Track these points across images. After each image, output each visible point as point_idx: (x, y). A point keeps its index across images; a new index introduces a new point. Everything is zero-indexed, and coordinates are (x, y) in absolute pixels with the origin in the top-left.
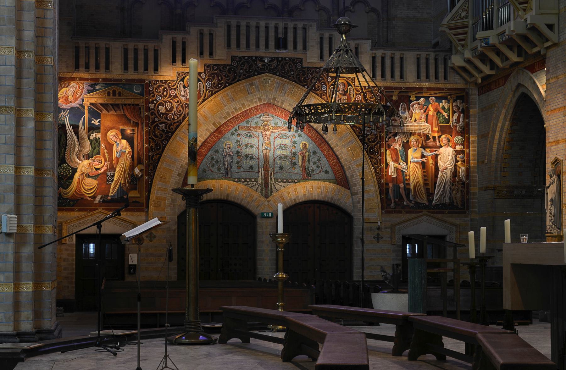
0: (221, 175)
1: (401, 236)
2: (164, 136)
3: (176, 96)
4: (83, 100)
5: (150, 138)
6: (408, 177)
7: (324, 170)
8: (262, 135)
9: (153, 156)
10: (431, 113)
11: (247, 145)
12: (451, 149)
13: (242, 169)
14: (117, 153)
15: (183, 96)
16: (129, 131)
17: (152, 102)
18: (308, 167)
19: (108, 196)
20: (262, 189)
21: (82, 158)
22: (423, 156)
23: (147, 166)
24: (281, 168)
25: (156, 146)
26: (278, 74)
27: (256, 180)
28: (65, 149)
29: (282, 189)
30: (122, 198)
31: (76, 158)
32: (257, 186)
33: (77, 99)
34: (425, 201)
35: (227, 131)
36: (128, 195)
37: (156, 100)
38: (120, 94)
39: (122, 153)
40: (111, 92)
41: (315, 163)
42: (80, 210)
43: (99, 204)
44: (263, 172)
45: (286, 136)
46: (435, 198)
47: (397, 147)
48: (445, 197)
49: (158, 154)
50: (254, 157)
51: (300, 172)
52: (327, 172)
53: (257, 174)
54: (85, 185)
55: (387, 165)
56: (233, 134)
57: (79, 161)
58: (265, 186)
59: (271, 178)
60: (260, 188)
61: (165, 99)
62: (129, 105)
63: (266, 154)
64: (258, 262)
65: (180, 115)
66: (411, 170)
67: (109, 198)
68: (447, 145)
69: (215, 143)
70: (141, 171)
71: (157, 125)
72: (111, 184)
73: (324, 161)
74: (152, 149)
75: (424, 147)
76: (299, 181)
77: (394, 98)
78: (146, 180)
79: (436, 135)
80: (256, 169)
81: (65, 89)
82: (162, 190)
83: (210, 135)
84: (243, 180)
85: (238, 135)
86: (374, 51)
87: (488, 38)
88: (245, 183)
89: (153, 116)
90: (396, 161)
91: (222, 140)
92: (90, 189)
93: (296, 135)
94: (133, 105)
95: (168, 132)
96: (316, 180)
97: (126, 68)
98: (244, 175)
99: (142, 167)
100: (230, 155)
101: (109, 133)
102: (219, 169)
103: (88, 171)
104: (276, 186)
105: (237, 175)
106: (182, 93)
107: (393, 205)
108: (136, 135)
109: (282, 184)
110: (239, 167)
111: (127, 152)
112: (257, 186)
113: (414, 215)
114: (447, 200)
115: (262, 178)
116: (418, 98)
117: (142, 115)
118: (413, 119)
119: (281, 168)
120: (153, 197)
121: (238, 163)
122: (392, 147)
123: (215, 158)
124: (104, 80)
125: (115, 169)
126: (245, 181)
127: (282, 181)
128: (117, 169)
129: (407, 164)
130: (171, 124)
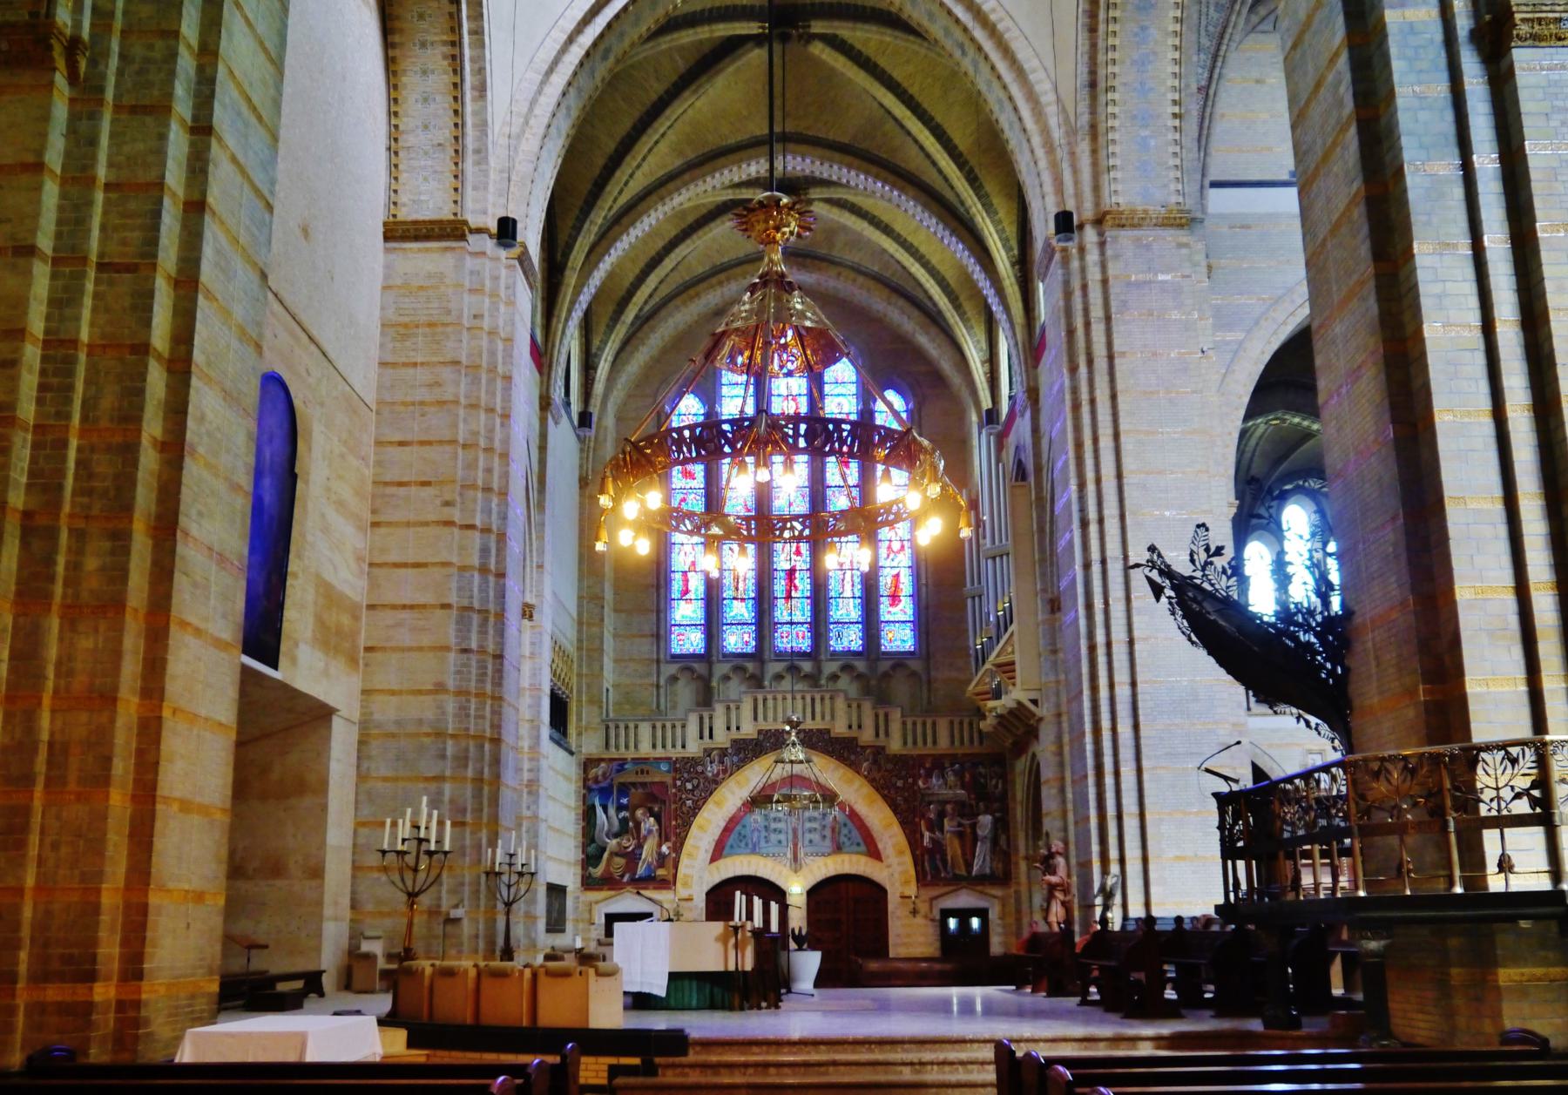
22: (960, 825)
23: (675, 844)
34: (964, 873)
39: (650, 832)
55: (922, 836)
68: (986, 812)
73: (855, 833)
75: (962, 816)
90: (931, 829)
97: (654, 746)
98: (771, 850)
114: (988, 871)
116: (952, 765)
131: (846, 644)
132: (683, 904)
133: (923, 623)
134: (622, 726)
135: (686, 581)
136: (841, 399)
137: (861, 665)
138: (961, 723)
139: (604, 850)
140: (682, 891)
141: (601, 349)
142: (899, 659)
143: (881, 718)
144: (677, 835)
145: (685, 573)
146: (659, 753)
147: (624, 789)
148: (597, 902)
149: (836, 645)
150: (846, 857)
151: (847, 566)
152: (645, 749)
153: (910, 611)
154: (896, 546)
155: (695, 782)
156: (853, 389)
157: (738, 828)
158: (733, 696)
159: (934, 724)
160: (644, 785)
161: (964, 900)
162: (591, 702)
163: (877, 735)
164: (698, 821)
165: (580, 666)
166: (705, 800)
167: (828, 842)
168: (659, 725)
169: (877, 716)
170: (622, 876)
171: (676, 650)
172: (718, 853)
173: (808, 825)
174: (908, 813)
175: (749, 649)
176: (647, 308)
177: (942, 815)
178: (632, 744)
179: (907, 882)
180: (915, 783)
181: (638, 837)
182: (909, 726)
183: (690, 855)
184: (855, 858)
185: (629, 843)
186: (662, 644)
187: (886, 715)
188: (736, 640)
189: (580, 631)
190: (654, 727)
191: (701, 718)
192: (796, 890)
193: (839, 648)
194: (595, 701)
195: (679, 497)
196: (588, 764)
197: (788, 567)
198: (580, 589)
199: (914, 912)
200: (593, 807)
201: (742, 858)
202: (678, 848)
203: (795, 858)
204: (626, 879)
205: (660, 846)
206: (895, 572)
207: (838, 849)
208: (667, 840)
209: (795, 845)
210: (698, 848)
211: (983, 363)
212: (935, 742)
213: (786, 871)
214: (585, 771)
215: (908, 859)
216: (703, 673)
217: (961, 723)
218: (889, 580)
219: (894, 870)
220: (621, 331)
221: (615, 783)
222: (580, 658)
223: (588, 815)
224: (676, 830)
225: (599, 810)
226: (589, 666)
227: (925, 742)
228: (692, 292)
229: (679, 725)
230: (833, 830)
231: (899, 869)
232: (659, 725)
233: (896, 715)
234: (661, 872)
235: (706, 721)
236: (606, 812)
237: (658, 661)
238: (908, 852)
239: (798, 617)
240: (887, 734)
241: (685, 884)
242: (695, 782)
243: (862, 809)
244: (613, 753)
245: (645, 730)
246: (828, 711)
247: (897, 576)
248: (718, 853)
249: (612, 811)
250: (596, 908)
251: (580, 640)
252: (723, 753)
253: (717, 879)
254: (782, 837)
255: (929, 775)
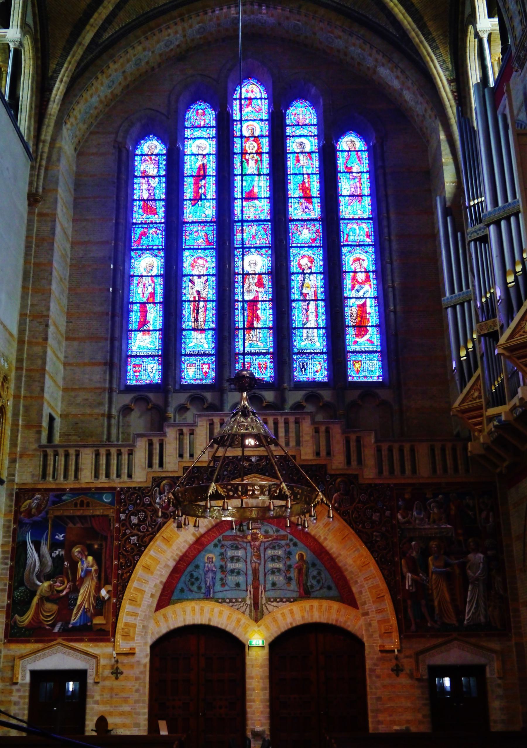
0: (202, 596)
1: (426, 667)
2: (136, 550)
3: (150, 505)
4: (47, 513)
5: (120, 553)
6: (430, 592)
7: (326, 585)
8: (251, 545)
9: (122, 575)
10: (453, 512)
11: (232, 558)
12: (482, 556)
13: (226, 588)
14: (82, 571)
15: (158, 504)
16: (96, 546)
17: (124, 512)
18: (306, 583)
19: (69, 623)
20: (251, 611)
21: (42, 579)
22: (447, 565)
23: (116, 587)
24: (274, 584)
25: (126, 563)
26: (267, 474)
27: (244, 600)
28: (24, 569)
29: (275, 609)
30: (85, 625)
31: (35, 579)
32: (245, 607)
33: (40, 512)
35: (209, 542)
36: (92, 622)
37: (128, 509)
38: (88, 505)
39: (88, 572)
40: (79, 502)
41: (314, 578)
42: (37, 642)
43: (59, 634)
44: (252, 590)
45: (278, 546)
46: (467, 618)
47: (414, 554)
48: (479, 615)
49: (129, 572)
50: (242, 572)
51: (296, 589)
52: (329, 588)
53: (245, 593)
54: (45, 611)
55: (404, 578)
56: (216, 546)
57: (39, 583)
58: (254, 607)
59: (262, 598)
60: (248, 609)
61: (139, 508)
62: (98, 516)
63: (255, 567)
64: (248, 704)
65: (155, 525)
66: (433, 582)
67: (70, 626)
68: (476, 551)
69: (195, 556)
70: (108, 592)
71: (129, 538)
72: (73, 609)
73: (325, 574)
74: (122, 567)
76: (295, 600)
77: (407, 496)
78: (114, 603)
79: (461, 538)
80: (243, 587)
81: (28, 502)
82: (132, 615)
83: (190, 548)
84: (228, 601)
85: (223, 546)
86: (379, 444)
87: (499, 415)
88: (231, 604)
89: (124, 528)
90: (414, 571)
91: (203, 553)
92: (50, 616)
93: (291, 544)
94: (102, 516)
95: (140, 546)
96: (316, 598)
98: (229, 595)
99: (110, 588)
100: (213, 571)
101: (74, 549)
102: (199, 588)
103: (47, 595)
104: (268, 606)
105: (220, 595)
106: (158, 500)
107: (413, 627)
108: (104, 550)
109: (275, 604)
110: (223, 585)
111: (93, 571)
112: (245, 607)
113: (440, 640)
115: (250, 598)
117: (112, 528)
118: (431, 520)
119: (274, 584)
120: (120, 625)
121: (221, 579)
122: (408, 555)
123: (195, 574)
124: (71, 489)
125: (78, 592)
126: (231, 601)
127: (275, 600)
128: (82, 591)
129: (428, 575)
130: (144, 537)
131: (310, 375)
132: (121, 659)
133: (389, 353)
134: (61, 451)
135: (144, 313)
136: (303, 140)
137: (326, 395)
138: (443, 449)
139: (34, 594)
140: (122, 644)
141: (57, 72)
142: (367, 387)
143: (353, 444)
144: (118, 577)
145: (143, 305)
146: (103, 482)
147: (60, 524)
148: (22, 657)
149: (300, 376)
150: (315, 603)
151: (311, 297)
152: (86, 477)
153: (376, 339)
154: (361, 277)
155: (142, 515)
156: (315, 131)
157: (190, 568)
158: (190, 420)
159: (412, 450)
160: (83, 518)
161: (455, 655)
162: (28, 426)
163: (349, 462)
164: (144, 560)
165: (18, 387)
166: (152, 536)
167: (294, 586)
168: (103, 451)
169: (348, 442)
170: (53, 626)
171: (132, 380)
172: (166, 598)
173: (271, 565)
174: (386, 552)
175: (209, 381)
176: (106, 36)
177: (425, 553)
178: (72, 473)
179: (387, 634)
180: (393, 516)
181: (74, 580)
182: (385, 453)
183: (133, 601)
184: (325, 603)
185: (63, 587)
186: (115, 373)
187: (358, 440)
188: (193, 372)
189: (20, 350)
190: (97, 455)
191: (151, 444)
192: (256, 640)
193: (303, 379)
194: (33, 426)
195: (139, 231)
196: (21, 495)
197: (249, 297)
198: (23, 306)
199: (397, 670)
200: (25, 543)
201: (193, 604)
202: (119, 592)
203: (256, 604)
204: (56, 630)
205: (98, 589)
206: (360, 302)
207: (306, 593)
208: (108, 582)
209: (256, 589)
210: (142, 592)
211: (450, 82)
212: (414, 470)
213: (245, 620)
214: (18, 503)
215: (388, 605)
216: (160, 403)
217: (443, 449)
218: (355, 311)
219: (371, 619)
220: (77, 53)
221: (51, 515)
222: (19, 379)
223: (18, 553)
224: (117, 573)
225: (31, 548)
226: (28, 387)
227: (403, 471)
228: (152, 24)
229: (125, 451)
230: (300, 570)
231: (379, 617)
232: (103, 451)
233: (370, 439)
234: (98, 620)
235: (157, 446)
236: (38, 550)
237: (111, 391)
238: (388, 597)
239: (260, 347)
240: (360, 461)
241: (127, 636)
242: (142, 515)
243: (331, 545)
244: (50, 483)
245: (87, 458)
246: (292, 435)
247: (364, 305)
248: (166, 598)
249: (45, 549)
250: (20, 663)
251: (19, 360)
252: (174, 481)
253: (164, 629)
254: (241, 579)
255: (408, 508)
